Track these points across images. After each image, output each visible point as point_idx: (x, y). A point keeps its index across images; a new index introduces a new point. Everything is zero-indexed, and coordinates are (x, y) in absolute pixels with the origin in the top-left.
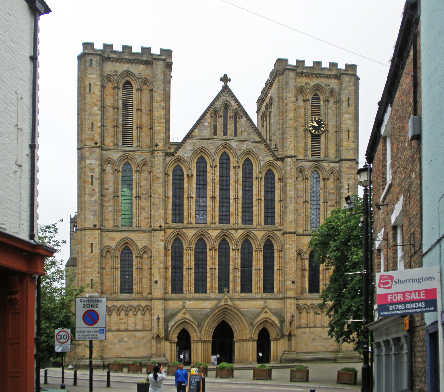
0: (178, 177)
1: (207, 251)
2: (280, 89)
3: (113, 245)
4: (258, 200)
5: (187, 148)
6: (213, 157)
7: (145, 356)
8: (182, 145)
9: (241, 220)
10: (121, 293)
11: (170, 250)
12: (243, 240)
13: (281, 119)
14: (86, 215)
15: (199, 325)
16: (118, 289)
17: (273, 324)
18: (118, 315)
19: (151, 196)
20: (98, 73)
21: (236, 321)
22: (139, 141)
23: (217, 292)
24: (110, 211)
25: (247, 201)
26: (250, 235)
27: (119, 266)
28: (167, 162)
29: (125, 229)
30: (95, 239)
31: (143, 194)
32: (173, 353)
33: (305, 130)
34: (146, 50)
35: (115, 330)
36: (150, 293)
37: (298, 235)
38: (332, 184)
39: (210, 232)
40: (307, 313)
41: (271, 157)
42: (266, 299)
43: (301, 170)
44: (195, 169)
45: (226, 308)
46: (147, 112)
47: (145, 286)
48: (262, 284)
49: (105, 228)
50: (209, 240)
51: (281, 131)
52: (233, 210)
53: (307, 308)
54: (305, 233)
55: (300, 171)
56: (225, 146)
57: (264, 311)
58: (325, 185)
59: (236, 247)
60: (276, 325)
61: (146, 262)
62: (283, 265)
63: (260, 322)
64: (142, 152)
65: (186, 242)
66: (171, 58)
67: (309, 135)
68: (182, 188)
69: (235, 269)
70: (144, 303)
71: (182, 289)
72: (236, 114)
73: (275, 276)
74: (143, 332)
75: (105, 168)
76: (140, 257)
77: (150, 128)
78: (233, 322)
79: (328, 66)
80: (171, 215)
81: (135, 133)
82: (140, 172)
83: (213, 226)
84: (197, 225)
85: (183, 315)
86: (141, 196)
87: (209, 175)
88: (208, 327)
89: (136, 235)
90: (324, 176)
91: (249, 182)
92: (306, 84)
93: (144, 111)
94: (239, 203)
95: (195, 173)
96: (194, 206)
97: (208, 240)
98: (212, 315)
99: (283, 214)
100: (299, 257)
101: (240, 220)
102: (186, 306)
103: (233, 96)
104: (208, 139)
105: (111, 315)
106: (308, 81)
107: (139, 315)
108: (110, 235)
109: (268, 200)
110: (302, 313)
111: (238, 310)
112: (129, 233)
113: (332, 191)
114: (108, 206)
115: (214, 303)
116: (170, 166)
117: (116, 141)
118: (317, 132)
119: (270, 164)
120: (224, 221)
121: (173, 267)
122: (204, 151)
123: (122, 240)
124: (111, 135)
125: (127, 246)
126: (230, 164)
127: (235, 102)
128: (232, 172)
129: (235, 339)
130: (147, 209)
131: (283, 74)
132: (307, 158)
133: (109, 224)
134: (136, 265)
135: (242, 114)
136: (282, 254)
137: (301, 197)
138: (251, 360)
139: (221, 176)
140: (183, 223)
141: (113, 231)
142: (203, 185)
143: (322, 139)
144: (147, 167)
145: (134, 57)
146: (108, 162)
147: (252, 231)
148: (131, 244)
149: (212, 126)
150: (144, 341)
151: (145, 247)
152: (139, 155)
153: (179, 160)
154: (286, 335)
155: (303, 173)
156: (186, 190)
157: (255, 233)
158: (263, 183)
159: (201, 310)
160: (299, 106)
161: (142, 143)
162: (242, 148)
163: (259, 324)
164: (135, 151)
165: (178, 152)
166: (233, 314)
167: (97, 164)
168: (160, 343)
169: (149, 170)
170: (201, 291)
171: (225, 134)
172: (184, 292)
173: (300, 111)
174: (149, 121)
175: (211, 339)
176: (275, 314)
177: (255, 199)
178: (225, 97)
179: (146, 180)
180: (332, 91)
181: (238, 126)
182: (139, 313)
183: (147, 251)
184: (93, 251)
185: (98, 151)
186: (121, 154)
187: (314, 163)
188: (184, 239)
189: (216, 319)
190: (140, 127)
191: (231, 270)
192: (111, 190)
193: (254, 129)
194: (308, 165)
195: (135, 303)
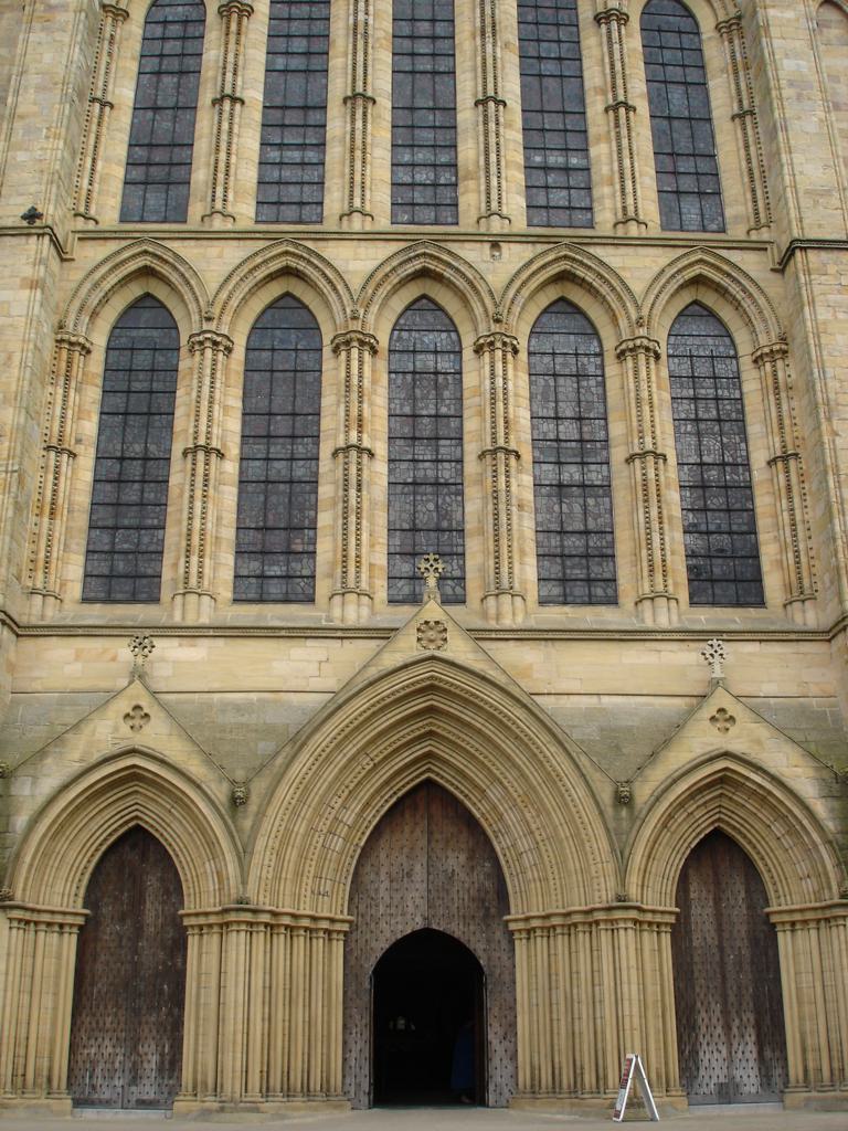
4: (615, 108)
21: (510, 778)
26: (581, 272)
39: (336, 253)
45: (431, 689)
50: (332, 297)
57: (710, 709)
59: (495, 328)
62: (805, 430)
65: (192, 306)
69: (496, 452)
73: (763, 502)
78: (494, 793)
88: (307, 812)
91: (559, 41)
94: (509, 125)
96: (249, 141)
97: (321, 294)
99: (762, 173)
136: (788, 371)
147: (591, 250)
158: (634, 42)
163: (681, 804)
166: (489, 729)
172: (165, 595)
177: (595, 107)
191: (471, 466)
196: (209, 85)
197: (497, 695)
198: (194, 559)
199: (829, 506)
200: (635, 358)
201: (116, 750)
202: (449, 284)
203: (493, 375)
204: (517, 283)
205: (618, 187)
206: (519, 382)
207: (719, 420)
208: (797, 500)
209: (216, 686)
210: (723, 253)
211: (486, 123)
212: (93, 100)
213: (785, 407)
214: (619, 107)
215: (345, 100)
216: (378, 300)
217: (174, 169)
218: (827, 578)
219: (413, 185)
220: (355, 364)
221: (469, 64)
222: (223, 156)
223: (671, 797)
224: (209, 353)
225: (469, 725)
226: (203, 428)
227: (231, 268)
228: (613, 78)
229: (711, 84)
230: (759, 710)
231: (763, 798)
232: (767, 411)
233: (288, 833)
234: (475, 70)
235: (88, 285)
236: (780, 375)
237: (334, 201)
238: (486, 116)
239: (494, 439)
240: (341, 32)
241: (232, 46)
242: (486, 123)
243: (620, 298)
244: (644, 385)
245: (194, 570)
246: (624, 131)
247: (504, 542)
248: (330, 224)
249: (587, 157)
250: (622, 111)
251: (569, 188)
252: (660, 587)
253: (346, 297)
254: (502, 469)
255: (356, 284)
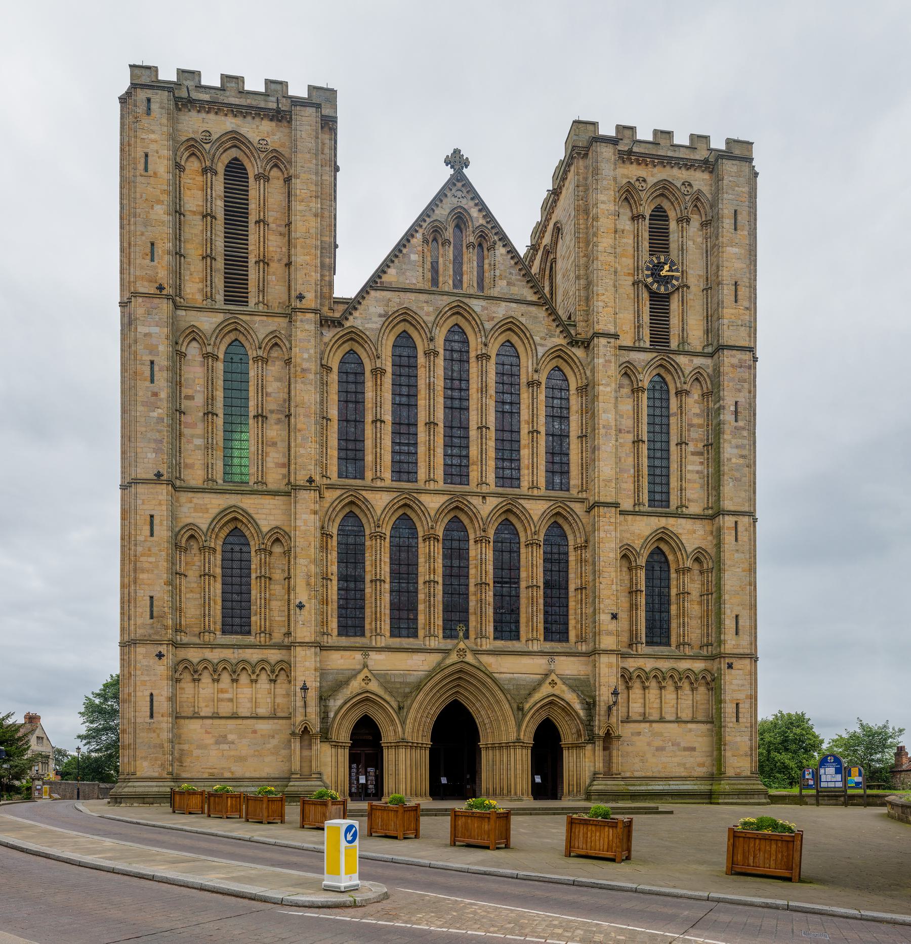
0: (351, 378)
1: (417, 543)
2: (581, 188)
3: (203, 521)
4: (532, 432)
5: (372, 309)
6: (431, 333)
7: (277, 776)
8: (360, 303)
9: (493, 475)
10: (224, 632)
11: (335, 538)
12: (500, 520)
13: (582, 254)
14: (139, 450)
15: (400, 708)
16: (215, 623)
17: (567, 710)
18: (214, 680)
19: (288, 416)
20: (165, 129)
21: (484, 701)
22: (262, 290)
23: (441, 635)
24: (198, 448)
25: (507, 436)
26: (515, 510)
27: (219, 571)
28: (326, 339)
29: (229, 488)
30: (160, 504)
31: (272, 412)
32: (341, 770)
33: (635, 283)
34: (276, 86)
35: (210, 715)
36: (288, 634)
37: (622, 513)
38: (697, 405)
39: (425, 498)
40: (645, 688)
41: (561, 336)
42: (552, 654)
43: (628, 371)
44: (390, 360)
45: (461, 671)
46: (283, 230)
47: (277, 618)
48: (542, 621)
49: (184, 485)
50: (423, 518)
51: (583, 282)
52: (475, 452)
53: (644, 677)
54: (637, 509)
55: (626, 373)
56: (459, 310)
57: (549, 680)
58: (681, 407)
60: (576, 712)
61: (278, 562)
62: (591, 578)
63: (539, 705)
64: (268, 315)
65: (371, 520)
66: (334, 107)
67: (646, 295)
68: (359, 403)
69: (481, 584)
70: (274, 656)
71: (363, 627)
72: (483, 236)
73: (572, 604)
74: (271, 721)
75: (183, 350)
76: (265, 550)
77: (286, 265)
78: (478, 705)
79: (687, 143)
80: (335, 461)
81: (253, 275)
82: (265, 361)
83: (432, 486)
84: (396, 485)
85: (363, 684)
86: (269, 415)
87: (422, 373)
89: (257, 501)
90: (679, 385)
91: (511, 394)
92: (638, 180)
93: (272, 226)
94: (490, 439)
95: (389, 369)
96: (387, 442)
98: (429, 685)
99: (588, 466)
100: (624, 562)
101: (491, 477)
102: (371, 663)
103: (475, 197)
104: (420, 291)
105: (199, 680)
106: (641, 172)
107: (263, 683)
108: (195, 501)
109: (553, 435)
110: (632, 687)
111: (490, 676)
112: (239, 496)
113: (696, 421)
114: (193, 436)
115: (435, 658)
116: (334, 349)
117: (209, 289)
118: (662, 289)
119: (558, 354)
120: (457, 479)
121: (342, 578)
122: (409, 318)
123: (224, 512)
124: (198, 276)
125: (236, 528)
126: (468, 352)
127: (480, 211)
128: (474, 368)
129: (482, 743)
130: (282, 446)
131: (586, 155)
132: (642, 345)
133: (195, 476)
134: (256, 569)
135: (496, 238)
136: (587, 555)
137: (628, 432)
138: (519, 792)
139: (448, 378)
140: (363, 478)
141: (202, 490)
142: (408, 396)
143: (675, 304)
144: (280, 352)
145: (249, 101)
146: (190, 337)
147: (520, 501)
148: (245, 521)
149: (428, 266)
150: (274, 742)
151: (277, 527)
152: (263, 321)
153: (354, 336)
154: (599, 737)
155: (633, 378)
156: (370, 405)
157: (527, 504)
158: (542, 397)
159: (405, 675)
160: (623, 231)
161: (269, 298)
162: (494, 315)
163: (537, 710)
164: (252, 314)
165: (351, 318)
167: (163, 336)
168: (310, 747)
169: (286, 357)
170: (404, 632)
171: (458, 283)
172: (368, 634)
173: (625, 240)
174: (285, 250)
175: (428, 741)
176: (573, 688)
177: (525, 430)
178: (457, 199)
179: (279, 380)
180: (698, 198)
181: (486, 267)
182: (263, 677)
183: (281, 538)
185: (165, 306)
186: (220, 317)
187: (656, 354)
188: (366, 515)
189: (438, 695)
190: (263, 261)
191: (472, 589)
192: (199, 400)
193: (523, 272)
194: (643, 360)
195: (253, 655)
196: (370, 412)
197: (482, 674)
198: (378, 622)
199: (595, 609)
200: (532, 547)
201: (360, 691)
202: (466, 513)
203: (481, 553)
204: (492, 514)
205: (531, 471)
206: (490, 555)
207: (559, 571)
208: (584, 605)
209: (389, 668)
210: (568, 503)
211: (482, 439)
212: (323, 418)
213: (583, 568)
214: (534, 432)
215: (426, 424)
216: (440, 520)
217: (358, 453)
218: (591, 634)
219: (452, 465)
220: (432, 547)
221: (475, 406)
222: (378, 450)
223: (535, 708)
224: (378, 540)
225: (472, 683)
226: (378, 572)
227: (385, 504)
228: (533, 417)
229: (571, 418)
230: (564, 680)
231: (563, 709)
232: (576, 569)
233: (416, 717)
234: (478, 410)
235: (331, 509)
236: (583, 555)
237: (422, 474)
238: (482, 435)
239: (481, 579)
240: (423, 386)
241: (379, 393)
242: (482, 439)
243: (529, 522)
244: (535, 559)
245: (378, 626)
246: (535, 445)
247: (484, 618)
248: (421, 484)
249: (519, 454)
250: (535, 434)
251: (511, 469)
252: (535, 636)
253: (429, 519)
254: (484, 591)
255: (432, 513)
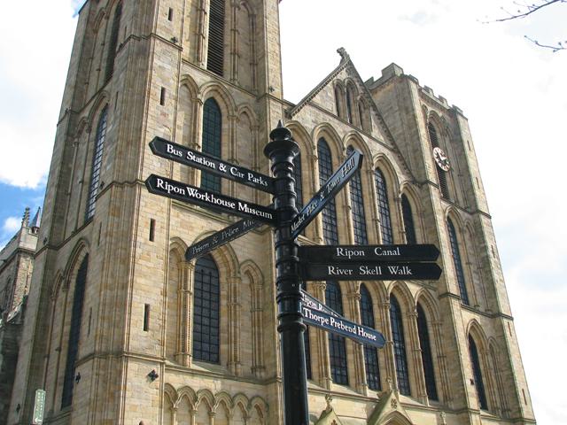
151: (250, 260)
156: (307, 180)
183: (252, 271)
184: (155, 238)
